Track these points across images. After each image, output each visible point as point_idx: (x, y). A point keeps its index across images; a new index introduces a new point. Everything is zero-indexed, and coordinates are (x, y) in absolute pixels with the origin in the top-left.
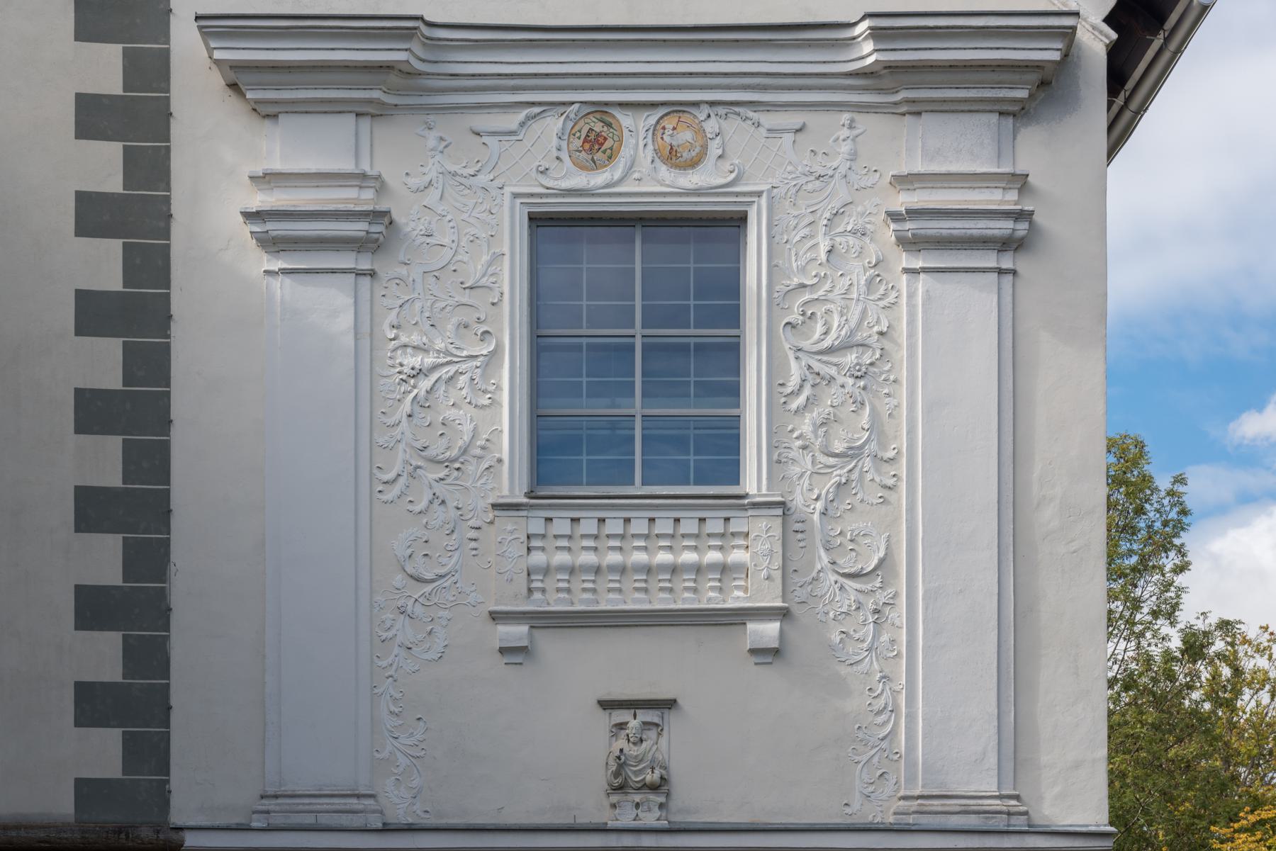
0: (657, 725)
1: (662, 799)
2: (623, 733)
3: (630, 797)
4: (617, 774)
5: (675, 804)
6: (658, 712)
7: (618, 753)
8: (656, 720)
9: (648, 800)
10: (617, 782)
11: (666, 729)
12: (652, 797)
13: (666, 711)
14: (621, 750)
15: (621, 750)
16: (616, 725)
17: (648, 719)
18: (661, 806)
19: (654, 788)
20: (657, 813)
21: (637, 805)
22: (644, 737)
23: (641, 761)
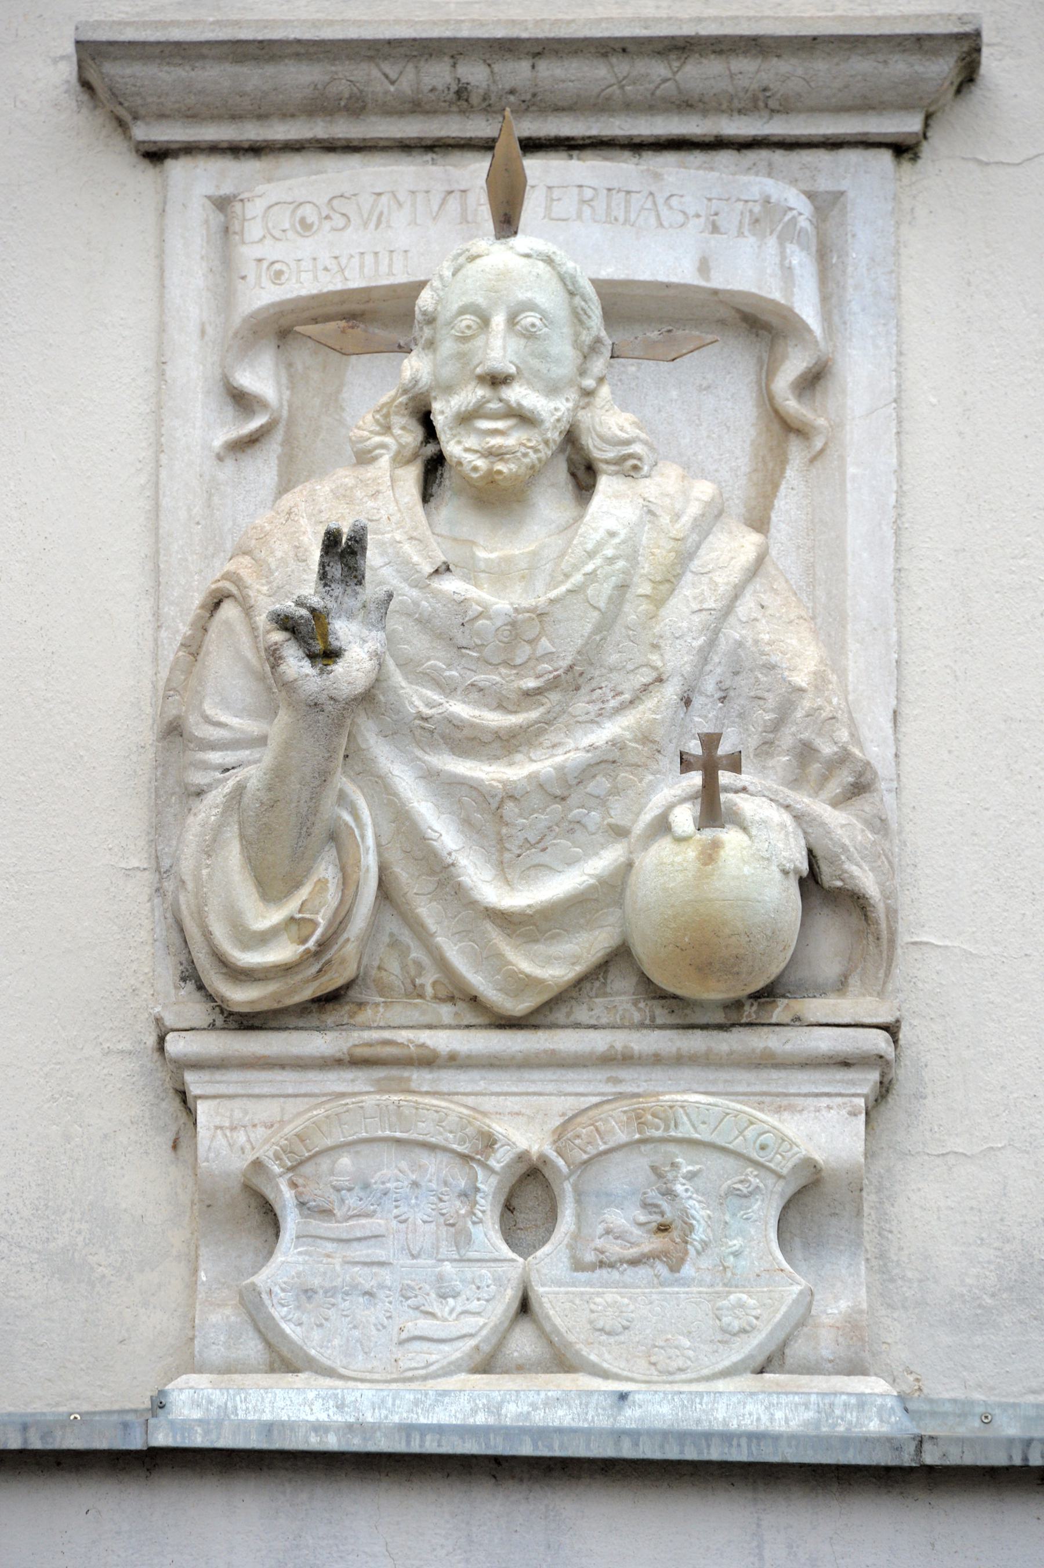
0: (758, 326)
1: (823, 1129)
2: (369, 393)
3: (440, 1106)
4: (288, 835)
5: (941, 1210)
6: (777, 186)
7: (303, 584)
8: (750, 269)
9: (654, 1135)
10: (264, 933)
11: (860, 372)
12: (695, 1102)
13: (867, 175)
14: (343, 553)
15: (343, 553)
16: (283, 329)
17: (664, 259)
18: (811, 1206)
19: (714, 996)
20: (756, 1277)
21: (529, 1196)
22: (610, 422)
23: (571, 681)
